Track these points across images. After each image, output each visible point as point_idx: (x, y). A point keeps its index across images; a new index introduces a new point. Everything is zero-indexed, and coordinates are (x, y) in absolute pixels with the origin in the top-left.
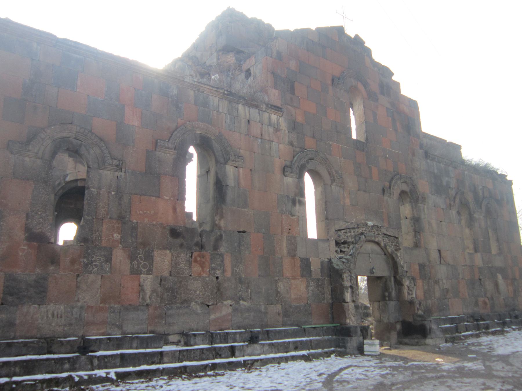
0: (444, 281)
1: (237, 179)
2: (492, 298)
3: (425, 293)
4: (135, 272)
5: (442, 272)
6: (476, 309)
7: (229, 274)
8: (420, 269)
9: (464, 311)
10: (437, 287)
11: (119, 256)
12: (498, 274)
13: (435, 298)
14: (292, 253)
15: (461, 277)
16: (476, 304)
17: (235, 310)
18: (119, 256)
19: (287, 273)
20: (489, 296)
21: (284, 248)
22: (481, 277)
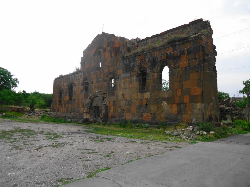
0: (123, 107)
1: (75, 90)
2: (154, 114)
3: (114, 111)
4: (65, 108)
5: (123, 103)
6: (140, 118)
7: (73, 107)
8: (113, 103)
9: (132, 118)
10: (119, 109)
11: (63, 105)
12: (163, 101)
13: (118, 113)
14: (81, 102)
15: (133, 104)
16: (141, 116)
17: (73, 114)
18: (63, 105)
19: (80, 106)
20: (152, 113)
21: (80, 101)
22: (148, 104)
